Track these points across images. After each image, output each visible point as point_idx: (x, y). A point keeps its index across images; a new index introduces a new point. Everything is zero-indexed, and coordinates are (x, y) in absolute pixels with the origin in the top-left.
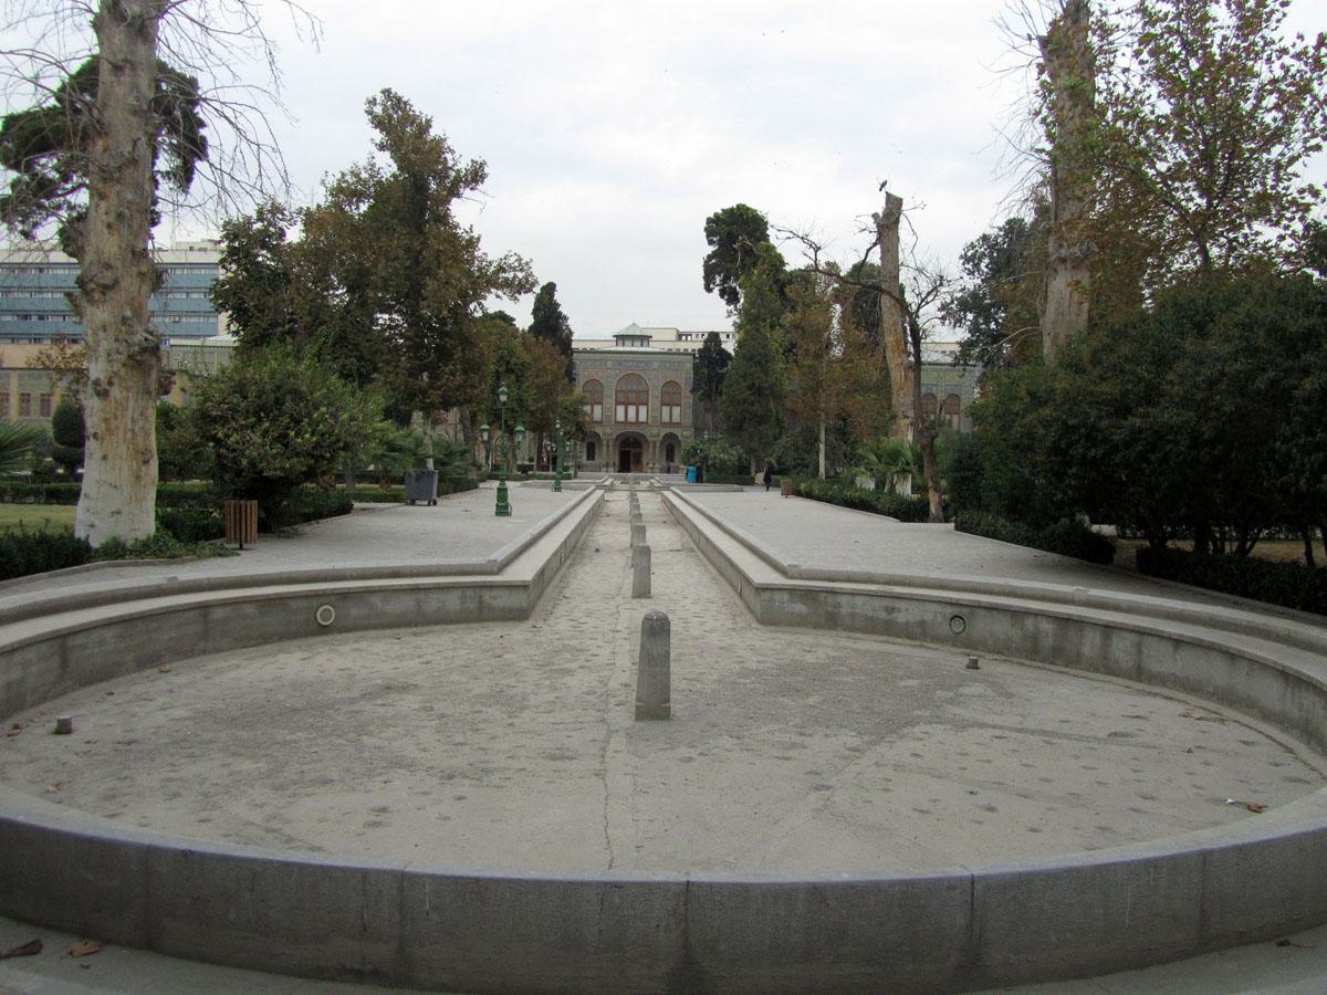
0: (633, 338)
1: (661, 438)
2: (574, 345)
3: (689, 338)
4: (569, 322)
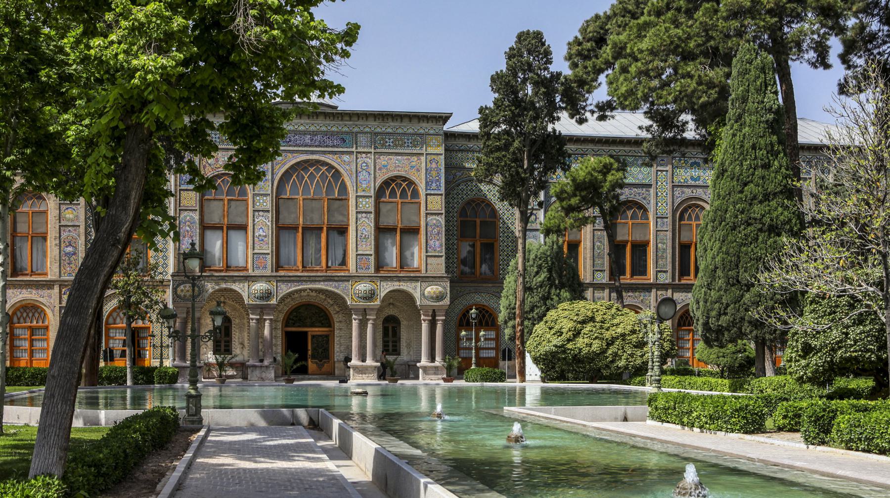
1: (378, 302)
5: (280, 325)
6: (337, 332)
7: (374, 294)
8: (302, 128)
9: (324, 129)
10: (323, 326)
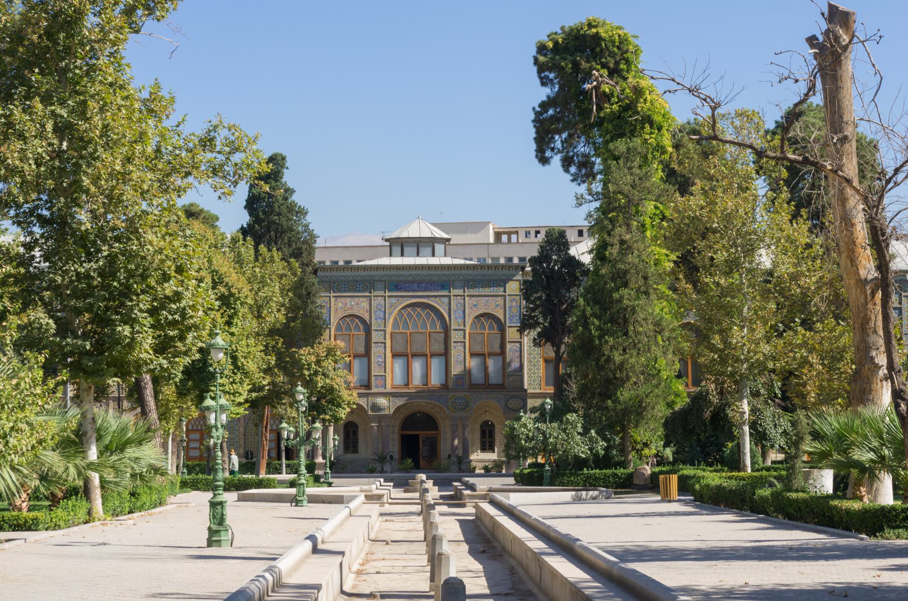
0: (419, 244)
2: (318, 257)
3: (514, 238)
4: (309, 218)
5: (397, 429)
6: (442, 434)
7: (467, 405)
8: (410, 278)
9: (428, 278)
10: (432, 430)
